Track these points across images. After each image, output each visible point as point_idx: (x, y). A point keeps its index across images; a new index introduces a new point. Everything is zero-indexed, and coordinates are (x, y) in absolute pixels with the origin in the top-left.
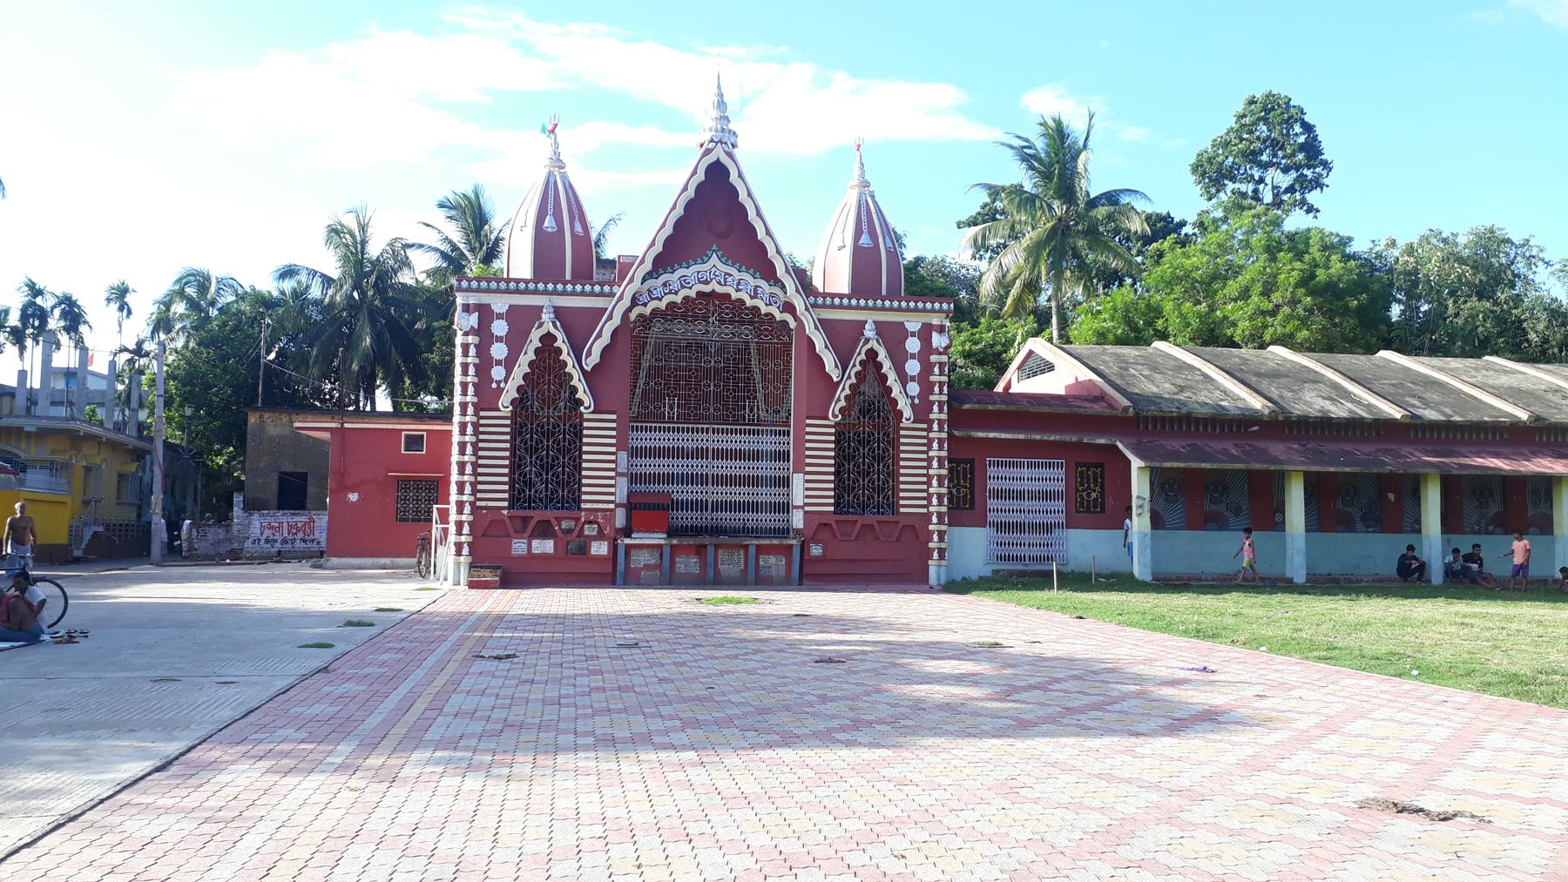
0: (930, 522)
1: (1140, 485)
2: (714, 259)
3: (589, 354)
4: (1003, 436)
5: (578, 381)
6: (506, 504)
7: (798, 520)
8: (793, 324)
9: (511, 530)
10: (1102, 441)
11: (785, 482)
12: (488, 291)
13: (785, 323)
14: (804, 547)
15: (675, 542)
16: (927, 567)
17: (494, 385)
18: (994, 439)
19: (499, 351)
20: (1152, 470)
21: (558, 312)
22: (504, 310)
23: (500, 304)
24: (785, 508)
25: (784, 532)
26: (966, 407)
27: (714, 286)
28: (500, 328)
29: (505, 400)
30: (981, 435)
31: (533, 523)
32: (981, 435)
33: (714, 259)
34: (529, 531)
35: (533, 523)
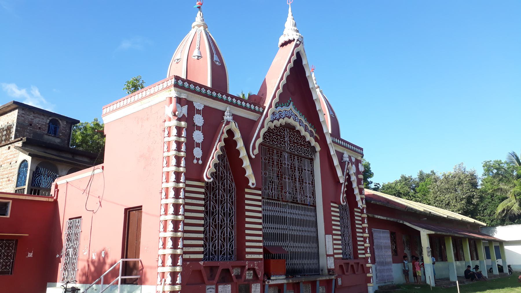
0: (368, 263)
1: (425, 242)
2: (291, 106)
3: (254, 148)
4: (382, 218)
5: (246, 163)
6: (201, 256)
7: (331, 264)
8: (318, 148)
9: (205, 279)
10: (401, 222)
11: (316, 239)
12: (194, 92)
13: (314, 148)
14: (336, 280)
15: (291, 281)
16: (367, 287)
17: (195, 161)
18: (379, 219)
19: (198, 136)
20: (430, 236)
21: (236, 118)
22: (201, 108)
23: (199, 103)
24: (317, 256)
25: (317, 271)
26: (372, 202)
27: (291, 121)
28: (199, 120)
29: (206, 175)
30: (379, 217)
31: (219, 270)
32: (379, 217)
33: (291, 106)
34: (217, 278)
35: (219, 270)
